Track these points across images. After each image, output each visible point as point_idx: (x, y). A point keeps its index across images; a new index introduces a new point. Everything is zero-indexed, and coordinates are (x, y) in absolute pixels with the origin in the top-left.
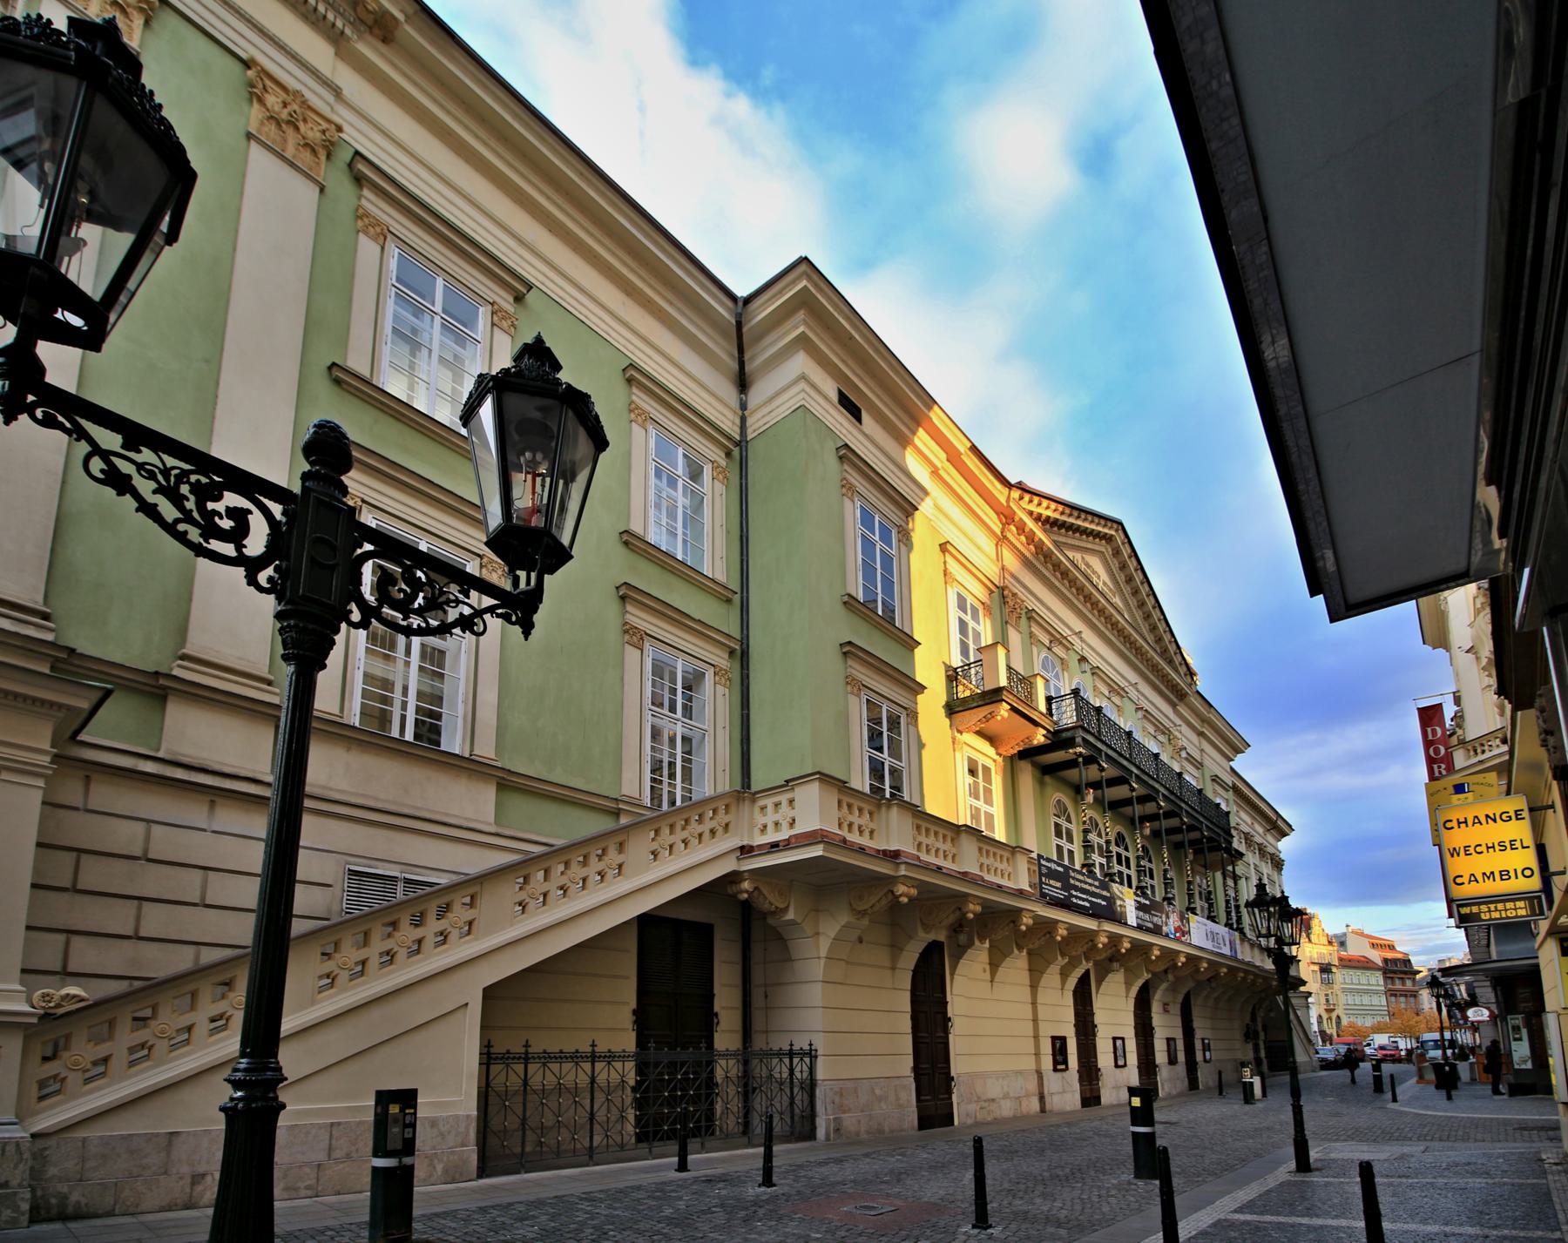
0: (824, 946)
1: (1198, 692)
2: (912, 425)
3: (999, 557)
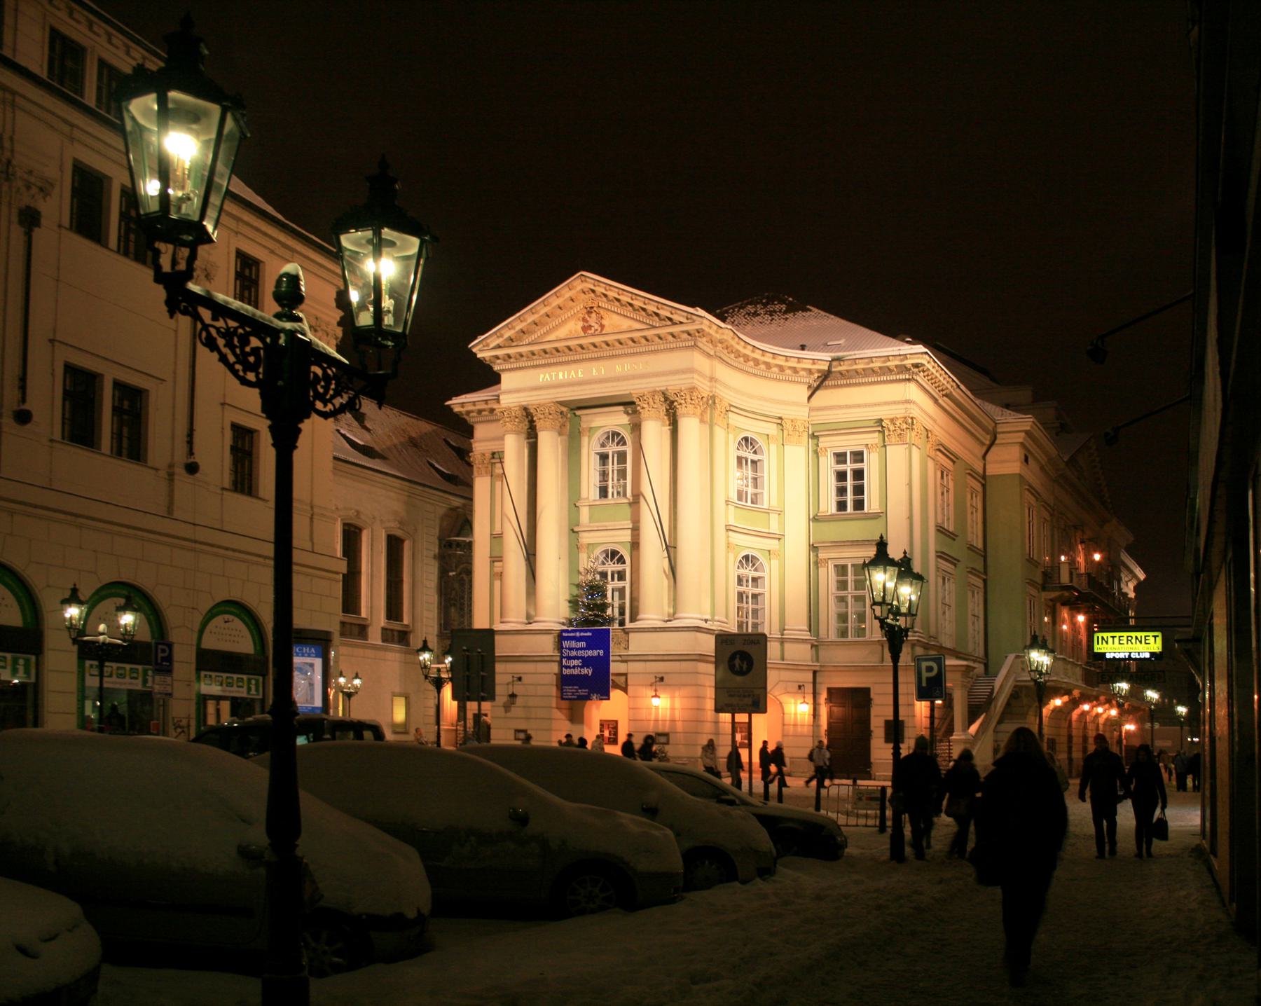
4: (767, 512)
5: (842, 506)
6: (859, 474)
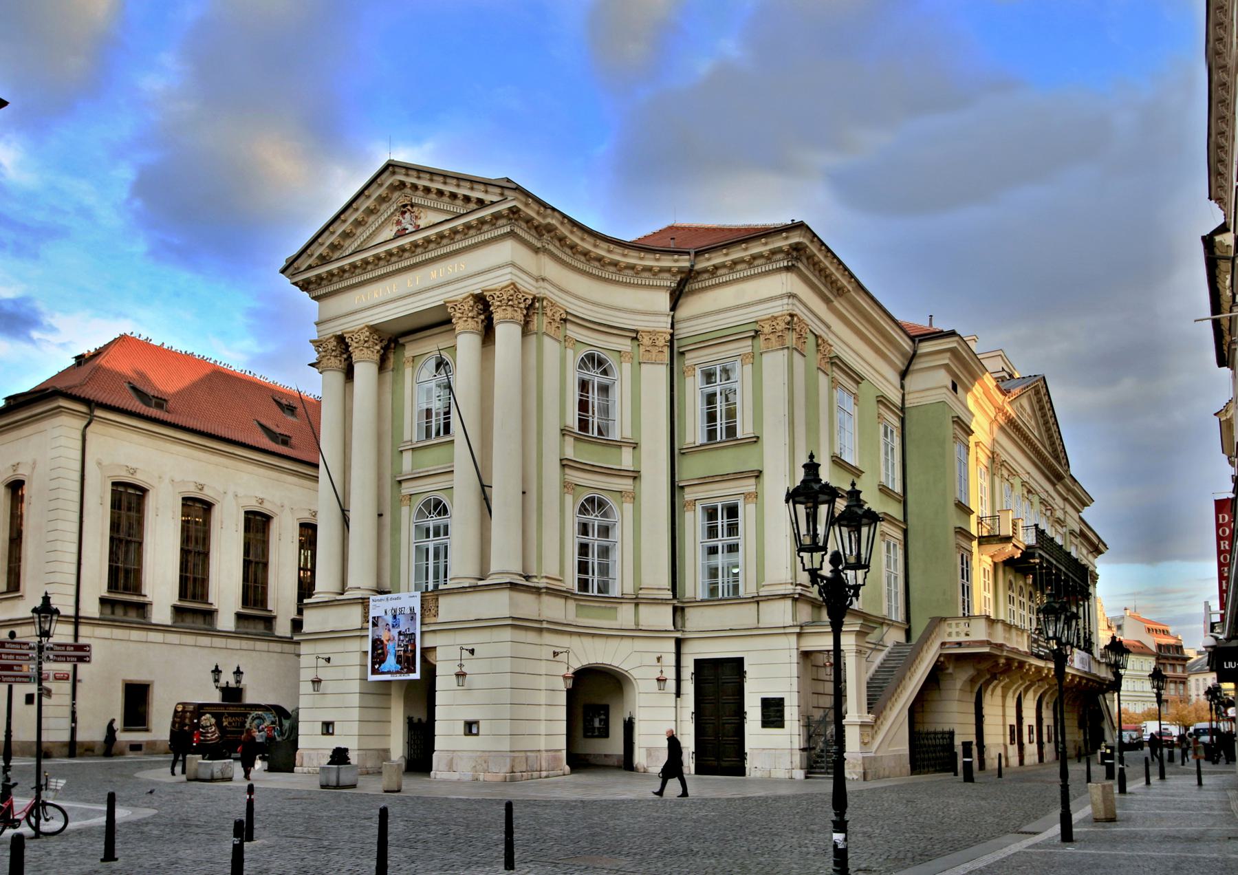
2: (971, 380)
4: (618, 445)
5: (711, 434)
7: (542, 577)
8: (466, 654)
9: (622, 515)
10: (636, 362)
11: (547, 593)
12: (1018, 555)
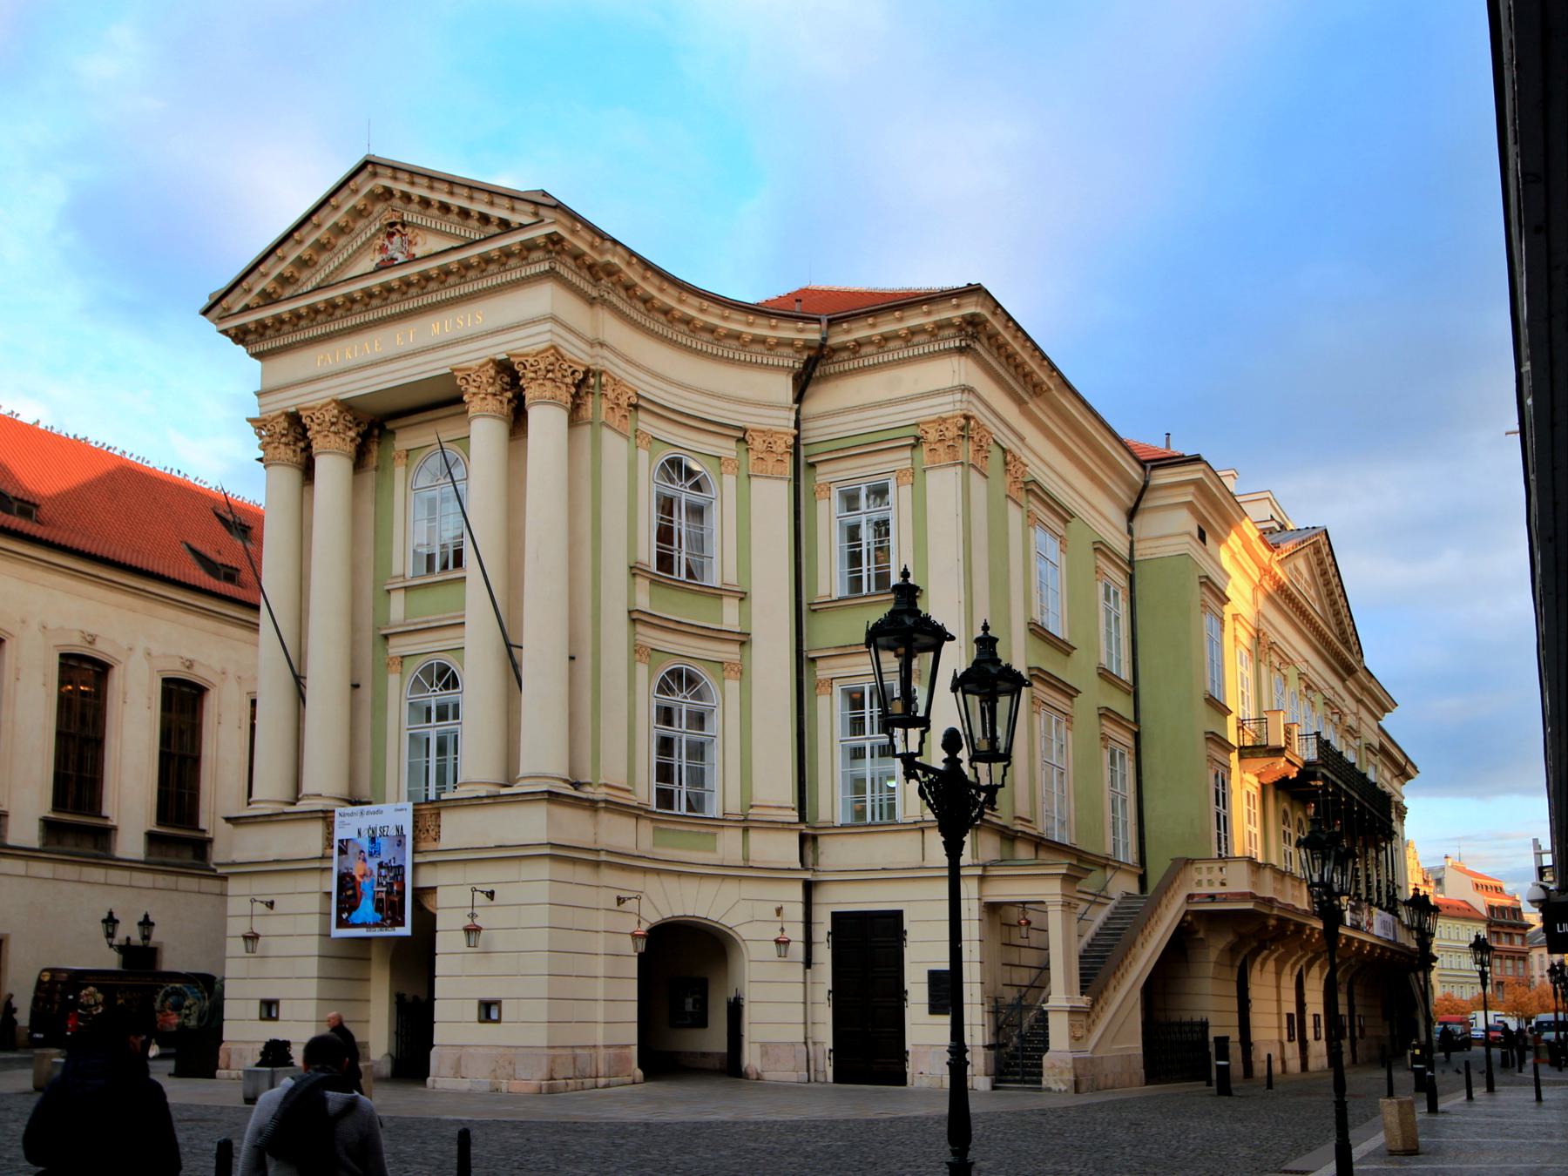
0: (1213, 954)
1: (1365, 668)
3: (1255, 602)
4: (718, 594)
5: (856, 583)
6: (882, 528)
7: (600, 785)
8: (481, 899)
9: (724, 699)
10: (743, 475)
11: (606, 809)
12: (1293, 774)
